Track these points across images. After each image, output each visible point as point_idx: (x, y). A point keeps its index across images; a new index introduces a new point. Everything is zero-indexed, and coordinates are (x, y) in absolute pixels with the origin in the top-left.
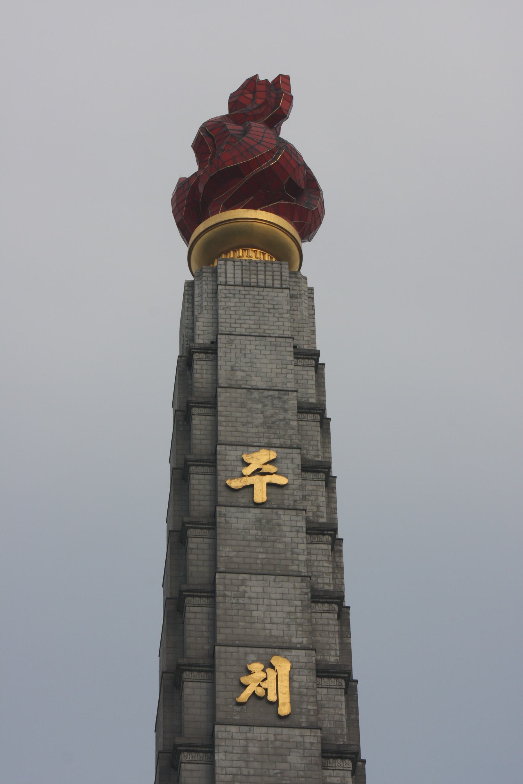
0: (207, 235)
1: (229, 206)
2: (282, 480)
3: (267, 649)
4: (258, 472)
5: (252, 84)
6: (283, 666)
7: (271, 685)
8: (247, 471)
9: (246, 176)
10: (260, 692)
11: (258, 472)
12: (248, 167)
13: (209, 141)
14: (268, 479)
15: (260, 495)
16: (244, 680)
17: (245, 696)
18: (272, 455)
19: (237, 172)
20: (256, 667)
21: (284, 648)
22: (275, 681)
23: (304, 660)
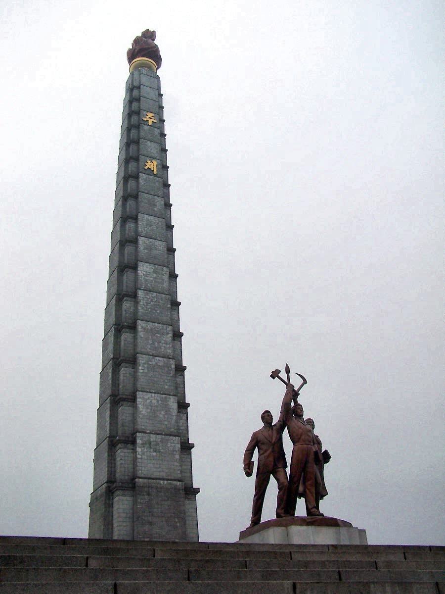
0: (138, 62)
1: (142, 57)
2: (155, 121)
3: (152, 158)
4: (150, 118)
5: (148, 31)
6: (155, 163)
7: (152, 166)
8: (147, 117)
9: (145, 50)
10: (150, 168)
11: (150, 118)
12: (149, 48)
13: (137, 41)
14: (152, 120)
15: (150, 123)
16: (146, 164)
17: (146, 168)
18: (153, 115)
19: (146, 49)
20: (149, 162)
21: (155, 159)
22: (153, 165)
23: (160, 163)
